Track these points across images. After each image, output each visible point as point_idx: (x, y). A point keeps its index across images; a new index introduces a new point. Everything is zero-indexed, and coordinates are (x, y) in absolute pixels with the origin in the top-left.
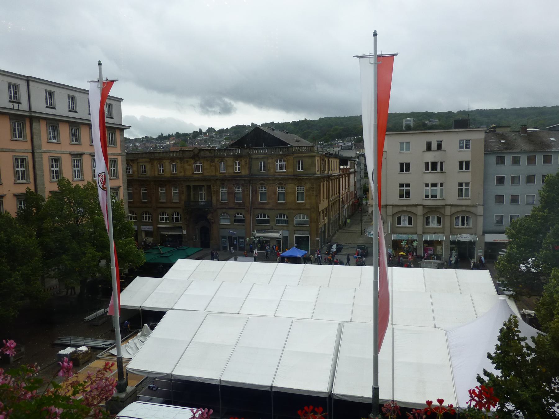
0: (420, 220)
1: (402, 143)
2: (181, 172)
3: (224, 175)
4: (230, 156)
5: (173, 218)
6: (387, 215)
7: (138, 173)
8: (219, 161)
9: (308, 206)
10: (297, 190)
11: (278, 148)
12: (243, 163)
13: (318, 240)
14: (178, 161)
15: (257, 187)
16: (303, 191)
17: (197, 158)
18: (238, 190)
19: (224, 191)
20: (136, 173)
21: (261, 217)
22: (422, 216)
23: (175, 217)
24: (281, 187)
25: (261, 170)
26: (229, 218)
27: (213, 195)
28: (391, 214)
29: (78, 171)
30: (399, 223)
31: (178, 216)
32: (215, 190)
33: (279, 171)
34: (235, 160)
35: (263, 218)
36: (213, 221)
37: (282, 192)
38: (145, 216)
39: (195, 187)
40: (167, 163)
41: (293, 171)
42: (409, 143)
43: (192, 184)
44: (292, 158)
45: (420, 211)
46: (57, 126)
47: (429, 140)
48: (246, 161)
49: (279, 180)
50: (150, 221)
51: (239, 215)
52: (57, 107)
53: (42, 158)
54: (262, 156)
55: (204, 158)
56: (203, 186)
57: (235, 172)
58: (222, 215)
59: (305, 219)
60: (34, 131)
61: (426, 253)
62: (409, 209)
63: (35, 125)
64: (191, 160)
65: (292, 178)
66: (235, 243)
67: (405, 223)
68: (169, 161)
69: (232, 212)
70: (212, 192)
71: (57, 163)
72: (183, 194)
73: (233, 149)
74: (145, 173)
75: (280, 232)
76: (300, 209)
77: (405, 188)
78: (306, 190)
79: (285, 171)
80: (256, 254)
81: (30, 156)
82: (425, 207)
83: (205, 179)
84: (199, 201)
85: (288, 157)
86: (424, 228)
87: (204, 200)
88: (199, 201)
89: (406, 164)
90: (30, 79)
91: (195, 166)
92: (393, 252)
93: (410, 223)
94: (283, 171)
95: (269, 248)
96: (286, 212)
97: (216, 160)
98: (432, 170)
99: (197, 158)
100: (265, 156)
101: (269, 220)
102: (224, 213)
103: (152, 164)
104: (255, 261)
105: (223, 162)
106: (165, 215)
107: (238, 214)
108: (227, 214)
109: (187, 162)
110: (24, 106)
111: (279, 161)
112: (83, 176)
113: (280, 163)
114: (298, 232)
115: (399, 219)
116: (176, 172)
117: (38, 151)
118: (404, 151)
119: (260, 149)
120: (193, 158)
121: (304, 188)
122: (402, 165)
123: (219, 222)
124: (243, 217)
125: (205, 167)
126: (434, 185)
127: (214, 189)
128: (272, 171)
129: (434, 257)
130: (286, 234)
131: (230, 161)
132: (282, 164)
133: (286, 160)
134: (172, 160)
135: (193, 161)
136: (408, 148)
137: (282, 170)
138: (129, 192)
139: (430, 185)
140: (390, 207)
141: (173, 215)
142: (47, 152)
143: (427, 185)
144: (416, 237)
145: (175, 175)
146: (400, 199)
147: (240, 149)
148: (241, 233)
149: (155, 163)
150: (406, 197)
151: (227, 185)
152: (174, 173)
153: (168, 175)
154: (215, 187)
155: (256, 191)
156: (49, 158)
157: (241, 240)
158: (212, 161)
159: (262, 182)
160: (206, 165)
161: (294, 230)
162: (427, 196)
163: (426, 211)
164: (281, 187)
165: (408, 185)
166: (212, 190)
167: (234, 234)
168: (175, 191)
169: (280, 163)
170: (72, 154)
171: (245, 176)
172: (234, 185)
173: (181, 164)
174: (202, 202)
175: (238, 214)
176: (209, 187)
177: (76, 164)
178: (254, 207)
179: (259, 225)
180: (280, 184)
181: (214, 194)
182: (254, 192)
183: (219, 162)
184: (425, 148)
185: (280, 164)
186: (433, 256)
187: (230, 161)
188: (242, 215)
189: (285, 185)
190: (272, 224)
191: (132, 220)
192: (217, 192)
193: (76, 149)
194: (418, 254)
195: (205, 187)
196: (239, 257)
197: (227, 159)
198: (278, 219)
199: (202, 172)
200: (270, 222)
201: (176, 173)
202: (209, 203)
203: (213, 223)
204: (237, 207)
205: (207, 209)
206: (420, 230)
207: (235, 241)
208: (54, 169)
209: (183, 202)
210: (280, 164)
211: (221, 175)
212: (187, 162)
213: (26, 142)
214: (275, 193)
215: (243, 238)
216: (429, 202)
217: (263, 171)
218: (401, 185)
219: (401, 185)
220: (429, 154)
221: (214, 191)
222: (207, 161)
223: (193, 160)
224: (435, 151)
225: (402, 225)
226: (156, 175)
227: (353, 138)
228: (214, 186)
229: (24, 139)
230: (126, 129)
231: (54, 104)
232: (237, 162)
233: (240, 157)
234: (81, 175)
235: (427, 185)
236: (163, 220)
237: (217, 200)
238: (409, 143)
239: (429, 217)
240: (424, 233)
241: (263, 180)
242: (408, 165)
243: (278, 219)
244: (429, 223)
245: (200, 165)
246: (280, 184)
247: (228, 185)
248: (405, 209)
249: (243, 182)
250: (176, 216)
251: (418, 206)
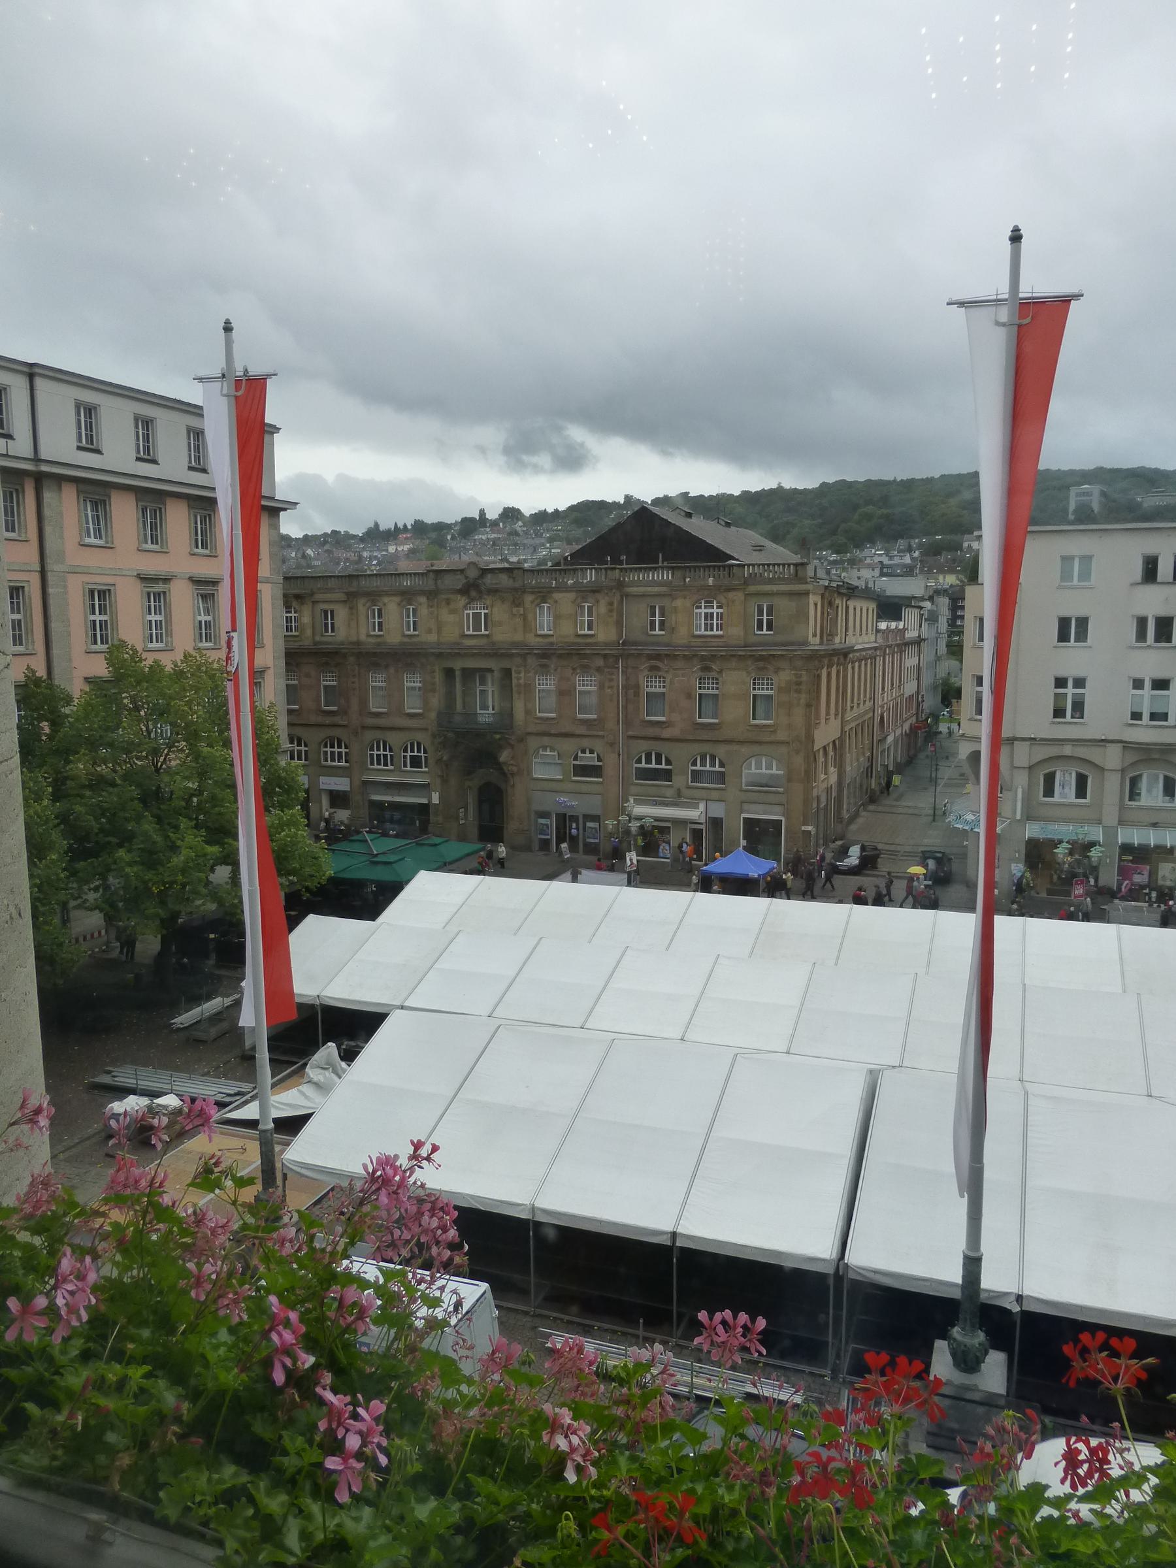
0: (1113, 785)
1: (1067, 560)
2: (430, 631)
3: (547, 640)
4: (567, 589)
5: (405, 757)
6: (1013, 767)
7: (314, 634)
8: (536, 603)
9: (781, 735)
10: (754, 689)
11: (703, 567)
12: (603, 609)
13: (809, 832)
14: (423, 599)
15: (641, 677)
16: (769, 692)
17: (473, 594)
18: (586, 685)
19: (547, 685)
20: (309, 632)
21: (648, 761)
22: (1119, 775)
23: (409, 754)
24: (709, 679)
25: (652, 628)
26: (559, 762)
27: (515, 695)
28: (1027, 765)
29: (158, 624)
30: (1049, 791)
31: (419, 751)
32: (522, 681)
33: (703, 632)
34: (579, 600)
35: (653, 765)
36: (515, 769)
37: (710, 692)
38: (382, 752)
39: (468, 674)
40: (392, 606)
41: (742, 633)
42: (1090, 557)
43: (458, 665)
44: (743, 598)
45: (1112, 758)
46: (105, 501)
47: (1151, 550)
48: (611, 604)
49: (703, 658)
50: (343, 764)
51: (587, 755)
52: (105, 447)
53: (65, 587)
54: (656, 589)
55: (494, 591)
56: (490, 670)
57: (580, 632)
58: (541, 752)
59: (774, 771)
60: (47, 512)
61: (1127, 882)
62: (1081, 752)
63: (48, 496)
65: (740, 653)
66: (574, 832)
67: (1066, 791)
68: (397, 599)
69: (569, 745)
70: (515, 689)
71: (160, 602)
72: (434, 691)
73: (577, 569)
74: (333, 630)
75: (702, 806)
76: (760, 743)
77: (1070, 691)
78: (780, 690)
79: (720, 633)
80: (632, 864)
81: (35, 580)
82: (1127, 746)
83: (496, 653)
84: (479, 711)
85: (731, 595)
86: (1122, 808)
87: (491, 711)
88: (479, 711)
89: (1077, 619)
90: (37, 370)
91: (468, 615)
92: (1028, 875)
93: (1081, 792)
94: (715, 632)
95: (668, 848)
96: (721, 751)
97: (528, 598)
98: (1157, 640)
99: (473, 594)
100: (664, 589)
101: (671, 770)
102: (545, 748)
103: (351, 608)
104: (629, 884)
105: (546, 605)
106: (385, 750)
107: (583, 751)
108: (552, 749)
109: (448, 602)
110: (21, 446)
111: (703, 605)
112: (172, 637)
113: (706, 611)
114: (753, 807)
115: (1050, 780)
116: (415, 629)
117: (56, 568)
118: (1072, 580)
119: (650, 569)
120: (465, 591)
121: (772, 684)
122: (1064, 623)
123: (529, 772)
124: (599, 759)
126: (1161, 684)
127: (518, 679)
128: (683, 631)
129: (1149, 894)
130: (717, 810)
131: (565, 600)
132: (712, 614)
133: (724, 601)
134: (407, 596)
135: (462, 601)
136: (1085, 575)
137: (712, 629)
139: (1148, 684)
140: (1024, 743)
141: (405, 751)
142: (79, 570)
143: (1138, 684)
144: (1097, 834)
145: (414, 640)
146: (1054, 723)
147: (595, 569)
148: (592, 805)
149: (362, 605)
150: (1073, 717)
151: (556, 670)
152: (411, 632)
153: (393, 638)
154: (522, 675)
155: (637, 686)
156: (84, 588)
157: (589, 824)
158: (517, 603)
159: (654, 662)
160: (500, 611)
161: (742, 802)
162: (1136, 716)
163: (1131, 758)
164: (709, 679)
165: (1080, 683)
166: (514, 681)
167: (572, 806)
168: (412, 681)
169: (706, 611)
170: (144, 579)
171: (606, 644)
172: (574, 669)
173: (432, 607)
174: (486, 716)
175: (583, 751)
176: (507, 673)
177: (152, 604)
178: (630, 733)
179: (641, 785)
180: (706, 669)
181: (519, 693)
182: (631, 692)
183: (538, 605)
184: (1138, 572)
185: (706, 614)
186: (1147, 891)
187: (565, 600)
188: (595, 755)
189: (720, 672)
190: (679, 781)
192: (528, 689)
193: (154, 565)
194: (1101, 883)
195: (496, 674)
196: (584, 872)
197: (556, 596)
198: (694, 768)
199: (487, 633)
200: (674, 777)
201: (417, 633)
202: (506, 717)
203: (513, 774)
204: (581, 730)
205: (498, 736)
206: (1110, 816)
207: (574, 825)
208: (98, 617)
209: (433, 715)
210: (706, 614)
211: (540, 640)
213: (163, 555)
214: (689, 696)
215: (596, 818)
216: (1145, 734)
217: (657, 632)
218: (1060, 682)
219: (1060, 682)
220: (1151, 590)
221: (519, 685)
222: (503, 600)
223: (464, 598)
224: (1169, 583)
225: (1057, 798)
226: (363, 638)
227: (917, 541)
228: (519, 673)
229: (162, 547)
230: (285, 509)
231: (98, 440)
232: (586, 605)
233: (594, 592)
234: (167, 636)
235: (1138, 684)
236: (379, 763)
237: (528, 712)
238: (1090, 557)
239: (1140, 776)
240: (1121, 822)
241: (658, 657)
242: (1083, 622)
243: (694, 768)
244: (1139, 794)
245: (483, 612)
246: (706, 669)
247: (559, 670)
248: (1068, 750)
249: (600, 662)
250: (412, 751)
251: (1108, 745)
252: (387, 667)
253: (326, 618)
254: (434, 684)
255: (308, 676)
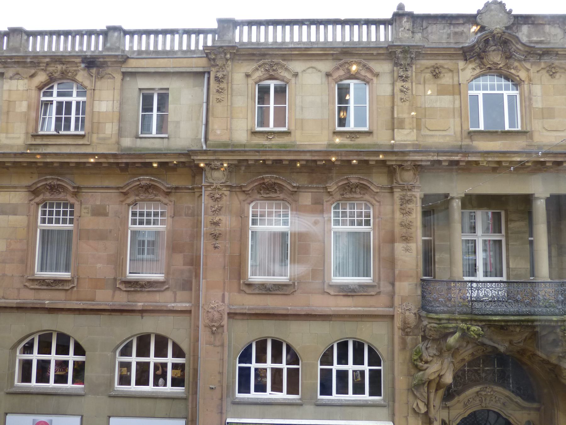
7: (120, 133)
20: (110, 129)
31: (358, 360)
50: (169, 389)
64: (461, 64)
68: (326, 66)
72: (406, 239)
74: (160, 129)
106: (277, 358)
109: (436, 74)
125: (540, 105)
138: (54, 226)
173: (405, 79)
191: (52, 384)
212: (436, 76)
223: (471, 66)
236: (277, 387)
245: (506, 93)
252: (295, 193)
253: (147, 108)
254: (407, 226)
255: (99, 212)
